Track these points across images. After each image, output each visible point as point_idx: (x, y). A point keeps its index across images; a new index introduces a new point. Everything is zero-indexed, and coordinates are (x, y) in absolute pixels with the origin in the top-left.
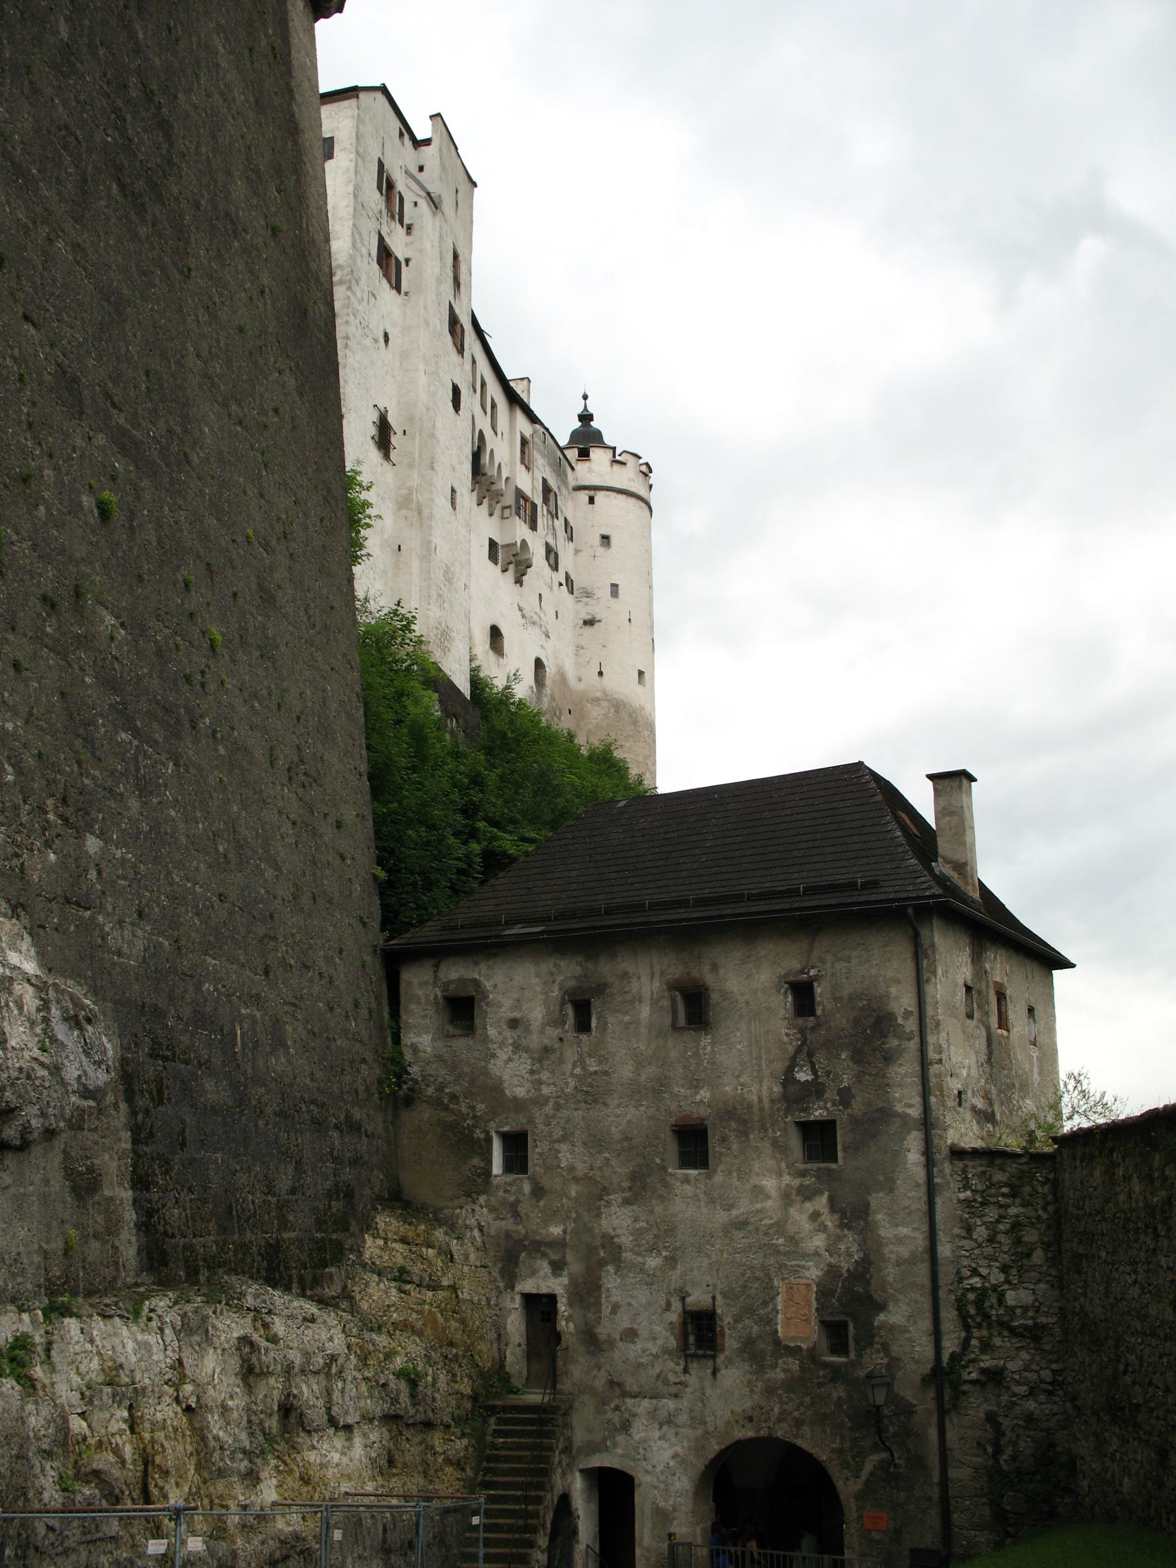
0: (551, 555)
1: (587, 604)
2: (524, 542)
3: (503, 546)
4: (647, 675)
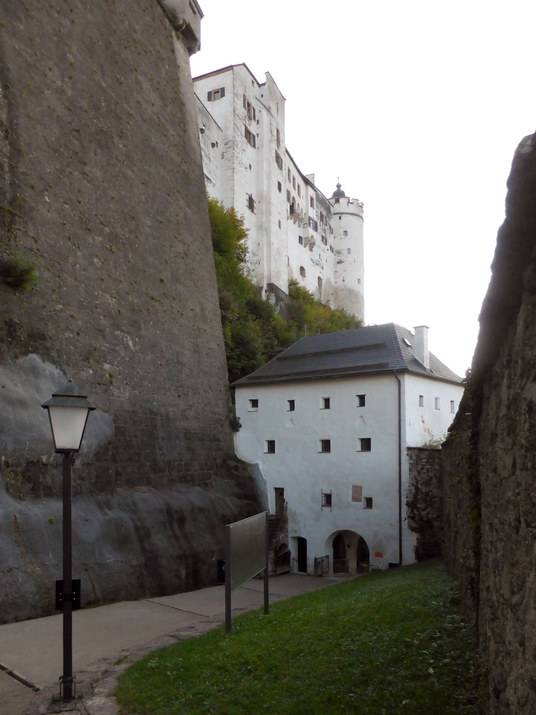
0: (324, 240)
1: (338, 256)
2: (312, 236)
3: (304, 238)
4: (361, 281)
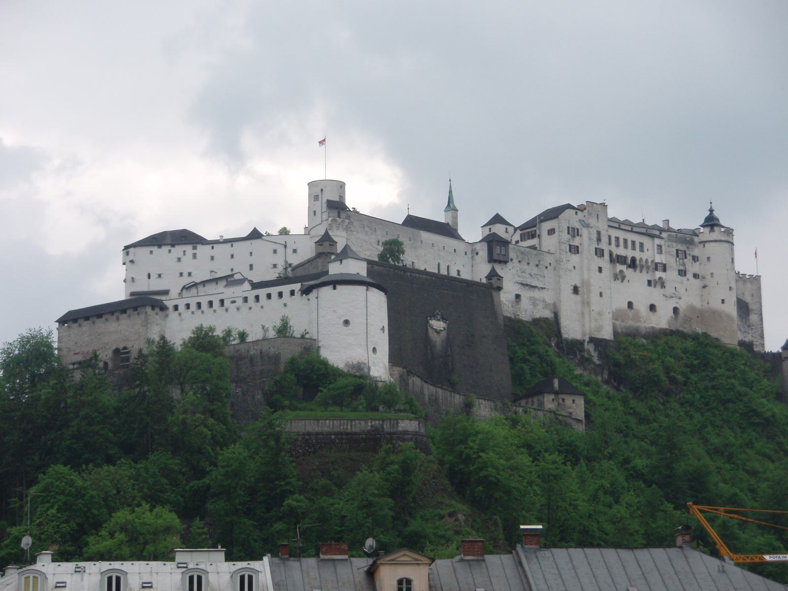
1: (703, 281)
